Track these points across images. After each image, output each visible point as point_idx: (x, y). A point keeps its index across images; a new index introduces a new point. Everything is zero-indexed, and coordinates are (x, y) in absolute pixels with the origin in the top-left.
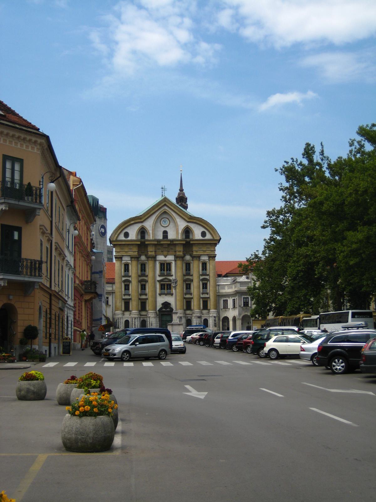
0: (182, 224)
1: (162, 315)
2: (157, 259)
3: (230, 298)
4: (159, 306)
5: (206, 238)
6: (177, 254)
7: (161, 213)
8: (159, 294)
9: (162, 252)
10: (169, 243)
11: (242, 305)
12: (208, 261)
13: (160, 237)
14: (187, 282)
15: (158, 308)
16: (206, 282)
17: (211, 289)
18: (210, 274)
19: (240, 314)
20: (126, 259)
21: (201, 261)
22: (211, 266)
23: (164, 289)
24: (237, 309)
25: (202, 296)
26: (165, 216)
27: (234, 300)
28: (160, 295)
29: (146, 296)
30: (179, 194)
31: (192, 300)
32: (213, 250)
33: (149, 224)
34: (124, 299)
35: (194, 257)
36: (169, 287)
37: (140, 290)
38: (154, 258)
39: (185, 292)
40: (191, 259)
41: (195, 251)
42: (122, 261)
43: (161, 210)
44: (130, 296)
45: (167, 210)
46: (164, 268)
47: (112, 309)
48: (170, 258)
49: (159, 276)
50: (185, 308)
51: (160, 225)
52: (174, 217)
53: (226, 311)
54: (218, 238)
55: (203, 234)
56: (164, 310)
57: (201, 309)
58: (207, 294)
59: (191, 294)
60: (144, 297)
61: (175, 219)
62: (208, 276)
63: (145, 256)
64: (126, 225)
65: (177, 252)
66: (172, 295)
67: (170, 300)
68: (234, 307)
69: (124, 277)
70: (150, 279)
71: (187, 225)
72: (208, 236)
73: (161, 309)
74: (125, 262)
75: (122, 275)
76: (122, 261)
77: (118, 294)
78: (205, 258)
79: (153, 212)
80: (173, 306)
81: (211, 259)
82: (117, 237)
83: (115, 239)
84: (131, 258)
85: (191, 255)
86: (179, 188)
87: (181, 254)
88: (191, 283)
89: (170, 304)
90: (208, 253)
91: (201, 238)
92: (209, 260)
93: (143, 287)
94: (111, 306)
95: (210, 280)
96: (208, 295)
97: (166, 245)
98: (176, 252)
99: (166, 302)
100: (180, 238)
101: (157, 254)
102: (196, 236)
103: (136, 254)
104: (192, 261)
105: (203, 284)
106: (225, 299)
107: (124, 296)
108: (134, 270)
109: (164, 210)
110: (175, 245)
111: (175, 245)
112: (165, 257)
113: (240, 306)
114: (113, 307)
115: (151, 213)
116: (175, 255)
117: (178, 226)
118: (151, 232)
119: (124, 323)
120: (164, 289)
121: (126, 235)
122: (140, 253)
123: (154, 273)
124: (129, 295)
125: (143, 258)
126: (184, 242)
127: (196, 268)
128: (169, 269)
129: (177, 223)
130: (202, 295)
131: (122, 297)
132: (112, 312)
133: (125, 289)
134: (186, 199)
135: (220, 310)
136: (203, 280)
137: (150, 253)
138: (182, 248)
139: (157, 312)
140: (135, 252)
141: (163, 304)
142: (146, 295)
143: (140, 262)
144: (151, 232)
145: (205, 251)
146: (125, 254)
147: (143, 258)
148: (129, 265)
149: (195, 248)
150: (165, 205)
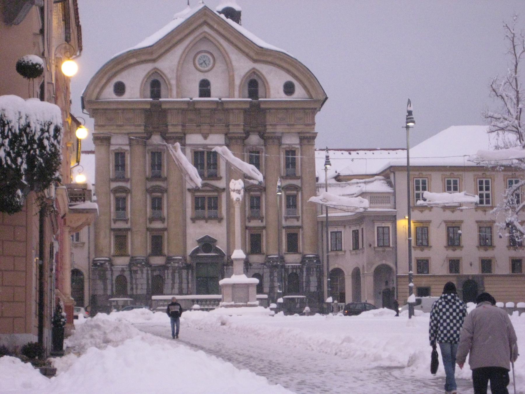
0: (242, 66)
2: (188, 142)
3: (347, 227)
6: (231, 131)
7: (195, 42)
9: (197, 126)
11: (374, 242)
12: (298, 146)
14: (252, 193)
16: (295, 192)
17: (304, 208)
18: (303, 176)
19: (370, 264)
20: (119, 142)
21: (284, 146)
23: (203, 208)
24: (363, 252)
25: (284, 223)
26: (204, 47)
27: (356, 234)
28: (194, 220)
29: (163, 222)
31: (264, 231)
32: (311, 122)
33: (168, 65)
34: (114, 230)
35: (269, 138)
37: (149, 209)
38: (182, 139)
39: (247, 214)
40: (262, 142)
41: (271, 125)
42: (109, 144)
43: (197, 33)
44: (127, 223)
45: (209, 35)
46: (202, 159)
47: (87, 252)
51: (193, 68)
52: (225, 51)
53: (337, 255)
54: (322, 98)
55: (289, 88)
57: (284, 251)
59: (261, 219)
60: (158, 225)
61: (227, 54)
62: (299, 181)
63: (161, 135)
64: (120, 67)
65: (231, 127)
67: (216, 231)
68: (356, 246)
71: (254, 69)
72: (299, 93)
73: (197, 251)
74: (117, 147)
75: (111, 177)
76: (109, 146)
78: (291, 141)
79: (179, 38)
80: (221, 245)
81: (305, 142)
82: (100, 93)
83: (93, 98)
85: (262, 136)
88: (262, 195)
89: (215, 241)
90: (300, 128)
91: (284, 97)
92: (301, 145)
93: (157, 204)
94: (86, 245)
95: (303, 188)
96: (298, 220)
98: (228, 126)
101: (186, 131)
102: (272, 92)
103: (141, 129)
104: (263, 147)
106: (336, 230)
107: (115, 223)
108: (137, 166)
109: (201, 34)
111: (227, 111)
112: (205, 138)
113: (370, 246)
114: (89, 248)
115: (175, 40)
116: (226, 134)
117: (233, 71)
118: (173, 82)
120: (203, 208)
121: (120, 89)
122: (150, 129)
124: (126, 221)
125: (156, 139)
129: (231, 63)
130: (286, 220)
131: (110, 225)
132: (89, 258)
133: (118, 209)
137: (171, 129)
138: (242, 116)
139: (188, 258)
140: (140, 125)
141: (199, 241)
142: (162, 220)
143: (150, 148)
144: (173, 82)
145: (293, 125)
146: (117, 131)
147: (156, 139)
148: (126, 154)
149: (270, 119)
150: (206, 23)
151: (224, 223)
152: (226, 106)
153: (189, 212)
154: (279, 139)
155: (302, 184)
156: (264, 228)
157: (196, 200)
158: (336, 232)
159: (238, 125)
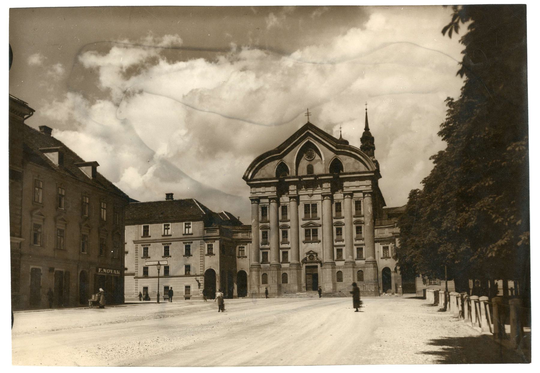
13: (303, 171)
25: (355, 242)
30: (364, 133)
33: (290, 159)
36: (315, 232)
38: (297, 199)
48: (317, 198)
49: (303, 220)
50: (335, 258)
58: (363, 239)
62: (363, 218)
70: (291, 224)
73: (306, 259)
86: (364, 127)
89: (317, 254)
99: (311, 251)
128: (315, 211)
134: (373, 139)
137: (291, 193)
141: (307, 254)
153: (302, 238)
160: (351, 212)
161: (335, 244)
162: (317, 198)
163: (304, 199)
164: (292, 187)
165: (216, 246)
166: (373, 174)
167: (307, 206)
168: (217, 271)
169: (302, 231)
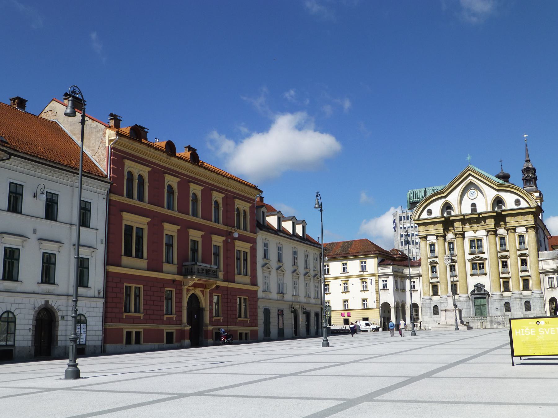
0: (491, 194)
1: (475, 298)
4: (471, 288)
5: (521, 206)
8: (471, 275)
10: (477, 216)
15: (470, 290)
20: (432, 239)
22: (530, 239)
23: (476, 269)
25: (521, 274)
28: (472, 275)
33: (453, 198)
34: (431, 283)
36: (482, 266)
38: (463, 235)
39: (501, 271)
48: (481, 233)
49: (470, 254)
50: (502, 289)
55: (517, 202)
56: (476, 292)
59: (508, 273)
66: (486, 274)
69: (430, 258)
73: (474, 291)
77: (425, 277)
80: (487, 288)
83: (416, 218)
84: (437, 237)
87: (492, 227)
89: (484, 286)
91: (515, 207)
97: (476, 219)
100: (490, 209)
103: (441, 231)
105: (522, 260)
106: (551, 276)
110: (485, 219)
112: (475, 232)
119: (432, 309)
120: (476, 269)
121: (429, 212)
123: (463, 250)
124: (437, 278)
125: (450, 236)
126: (495, 214)
127: (512, 241)
135: (546, 289)
136: (521, 255)
137: (456, 230)
138: (493, 220)
141: (475, 286)
149: (508, 219)
150: (470, 175)
151: (488, 275)
152: (484, 215)
154: (515, 230)
155: (529, 252)
156: (510, 277)
157: (473, 264)
158: (551, 278)
159: (491, 224)
160: (516, 246)
161: (501, 276)
162: (481, 233)
163: (469, 234)
164: (457, 225)
165: (390, 281)
166: (534, 210)
167: (472, 241)
168: (392, 305)
169: (468, 265)
